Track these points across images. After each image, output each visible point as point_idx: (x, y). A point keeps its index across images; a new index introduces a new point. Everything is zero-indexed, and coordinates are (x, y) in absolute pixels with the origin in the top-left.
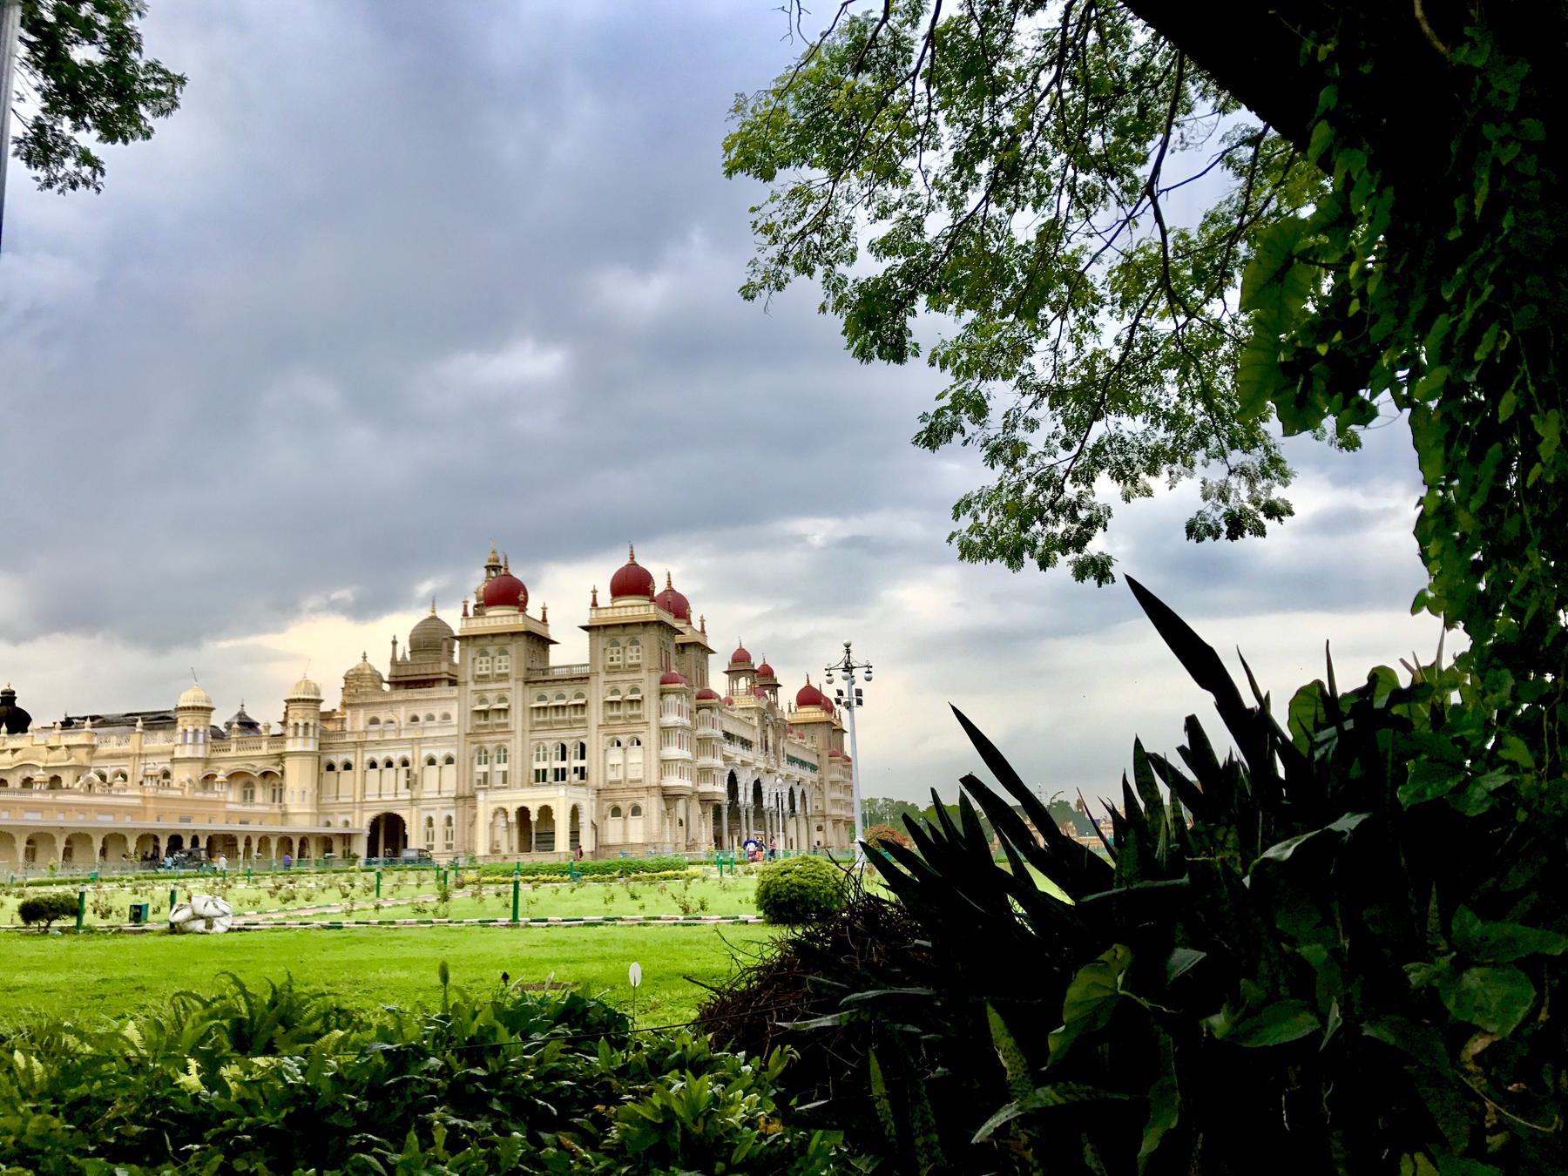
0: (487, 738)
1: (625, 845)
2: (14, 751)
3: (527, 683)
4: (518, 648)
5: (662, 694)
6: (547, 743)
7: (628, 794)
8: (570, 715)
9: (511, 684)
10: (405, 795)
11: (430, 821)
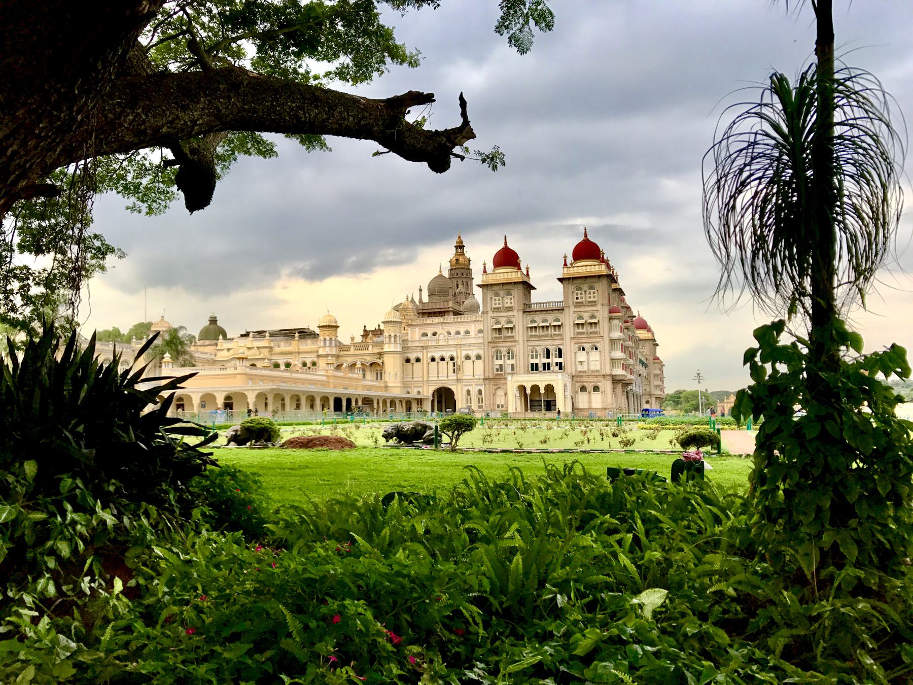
0: (501, 345)
1: (590, 409)
2: (229, 350)
3: (524, 312)
4: (518, 292)
6: (538, 348)
7: (591, 379)
8: (551, 331)
9: (515, 313)
10: (453, 377)
11: (469, 392)
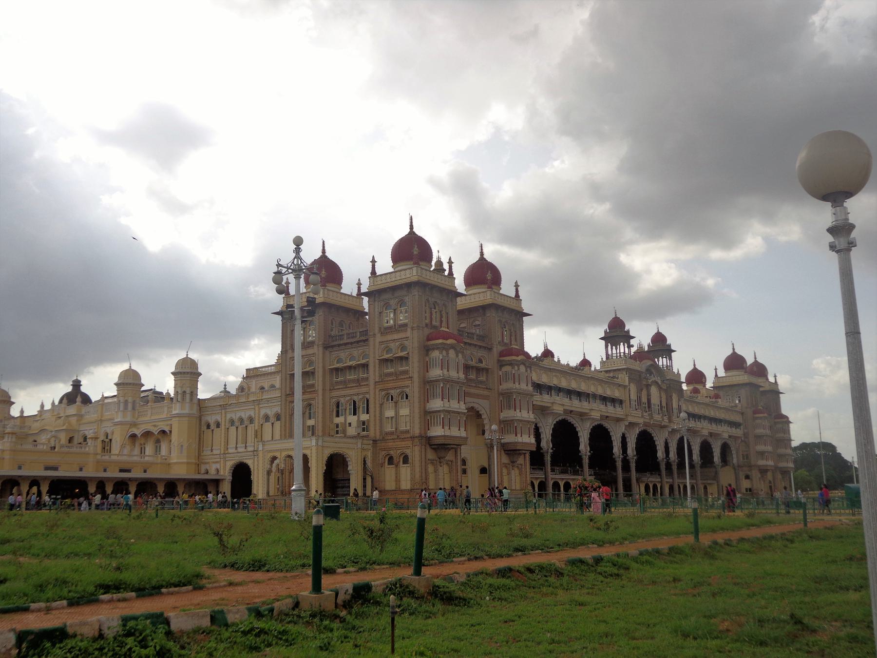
5: (427, 350)
6: (342, 400)
7: (399, 444)
